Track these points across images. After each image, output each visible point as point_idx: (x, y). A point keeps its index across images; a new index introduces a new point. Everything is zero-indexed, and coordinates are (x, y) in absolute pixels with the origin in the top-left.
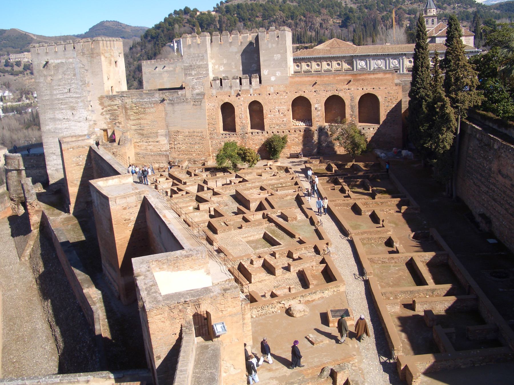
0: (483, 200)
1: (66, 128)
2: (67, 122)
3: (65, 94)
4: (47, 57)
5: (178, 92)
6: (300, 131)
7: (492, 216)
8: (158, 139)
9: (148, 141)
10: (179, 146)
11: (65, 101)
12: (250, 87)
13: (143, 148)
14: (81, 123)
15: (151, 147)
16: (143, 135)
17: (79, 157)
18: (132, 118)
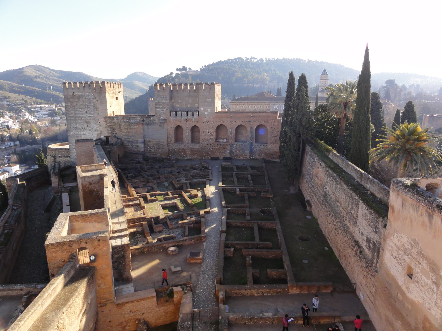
0: (309, 192)
1: (83, 134)
2: (84, 131)
5: (151, 118)
7: (312, 202)
10: (150, 149)
11: (84, 118)
12: (193, 118)
13: (129, 149)
14: (93, 132)
16: (129, 141)
18: (123, 131)
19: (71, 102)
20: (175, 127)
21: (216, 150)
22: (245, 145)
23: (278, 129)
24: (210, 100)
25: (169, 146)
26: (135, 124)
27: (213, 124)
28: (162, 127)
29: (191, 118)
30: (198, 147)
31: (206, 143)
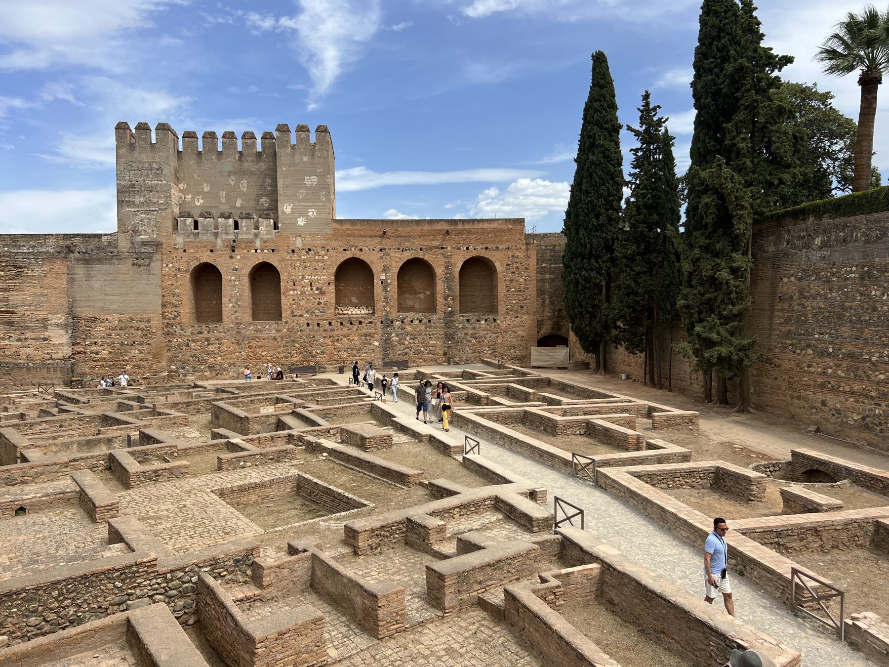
6: (351, 323)
8: (47, 334)
9: (23, 337)
10: (94, 348)
13: (8, 353)
15: (28, 351)
16: (10, 323)
20: (191, 269)
21: (338, 340)
22: (430, 321)
23: (527, 268)
24: (315, 179)
25: (168, 334)
26: (36, 259)
27: (326, 257)
28: (141, 269)
29: (251, 237)
30: (273, 333)
31: (303, 321)
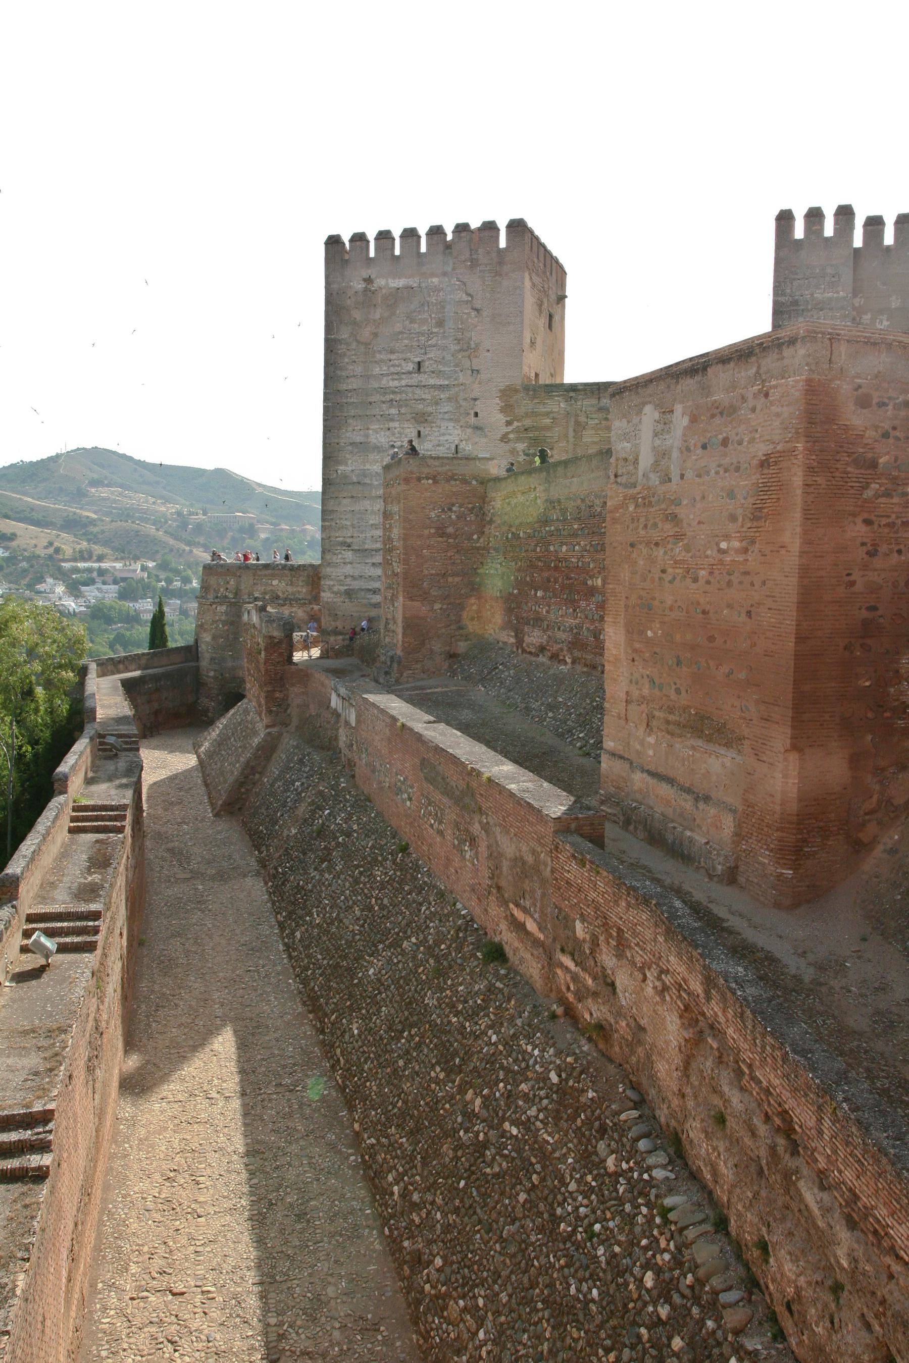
3: (404, 376)
4: (369, 271)
17: (450, 509)
19: (355, 323)
